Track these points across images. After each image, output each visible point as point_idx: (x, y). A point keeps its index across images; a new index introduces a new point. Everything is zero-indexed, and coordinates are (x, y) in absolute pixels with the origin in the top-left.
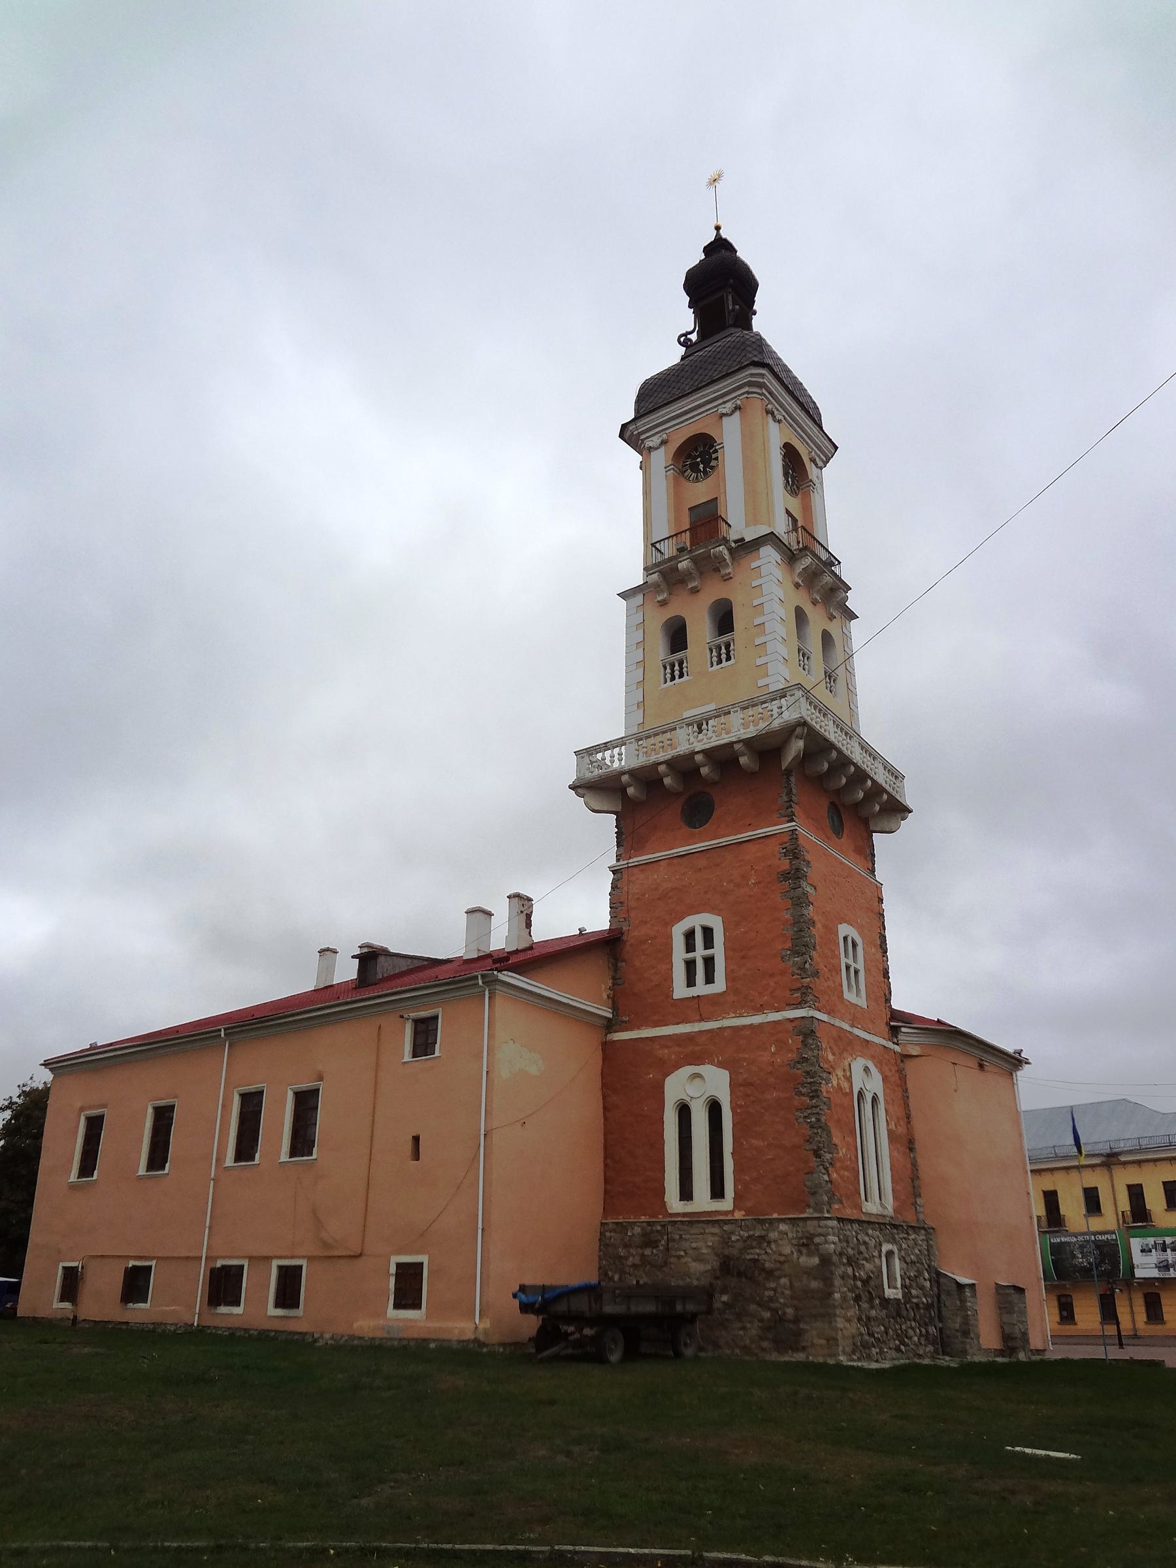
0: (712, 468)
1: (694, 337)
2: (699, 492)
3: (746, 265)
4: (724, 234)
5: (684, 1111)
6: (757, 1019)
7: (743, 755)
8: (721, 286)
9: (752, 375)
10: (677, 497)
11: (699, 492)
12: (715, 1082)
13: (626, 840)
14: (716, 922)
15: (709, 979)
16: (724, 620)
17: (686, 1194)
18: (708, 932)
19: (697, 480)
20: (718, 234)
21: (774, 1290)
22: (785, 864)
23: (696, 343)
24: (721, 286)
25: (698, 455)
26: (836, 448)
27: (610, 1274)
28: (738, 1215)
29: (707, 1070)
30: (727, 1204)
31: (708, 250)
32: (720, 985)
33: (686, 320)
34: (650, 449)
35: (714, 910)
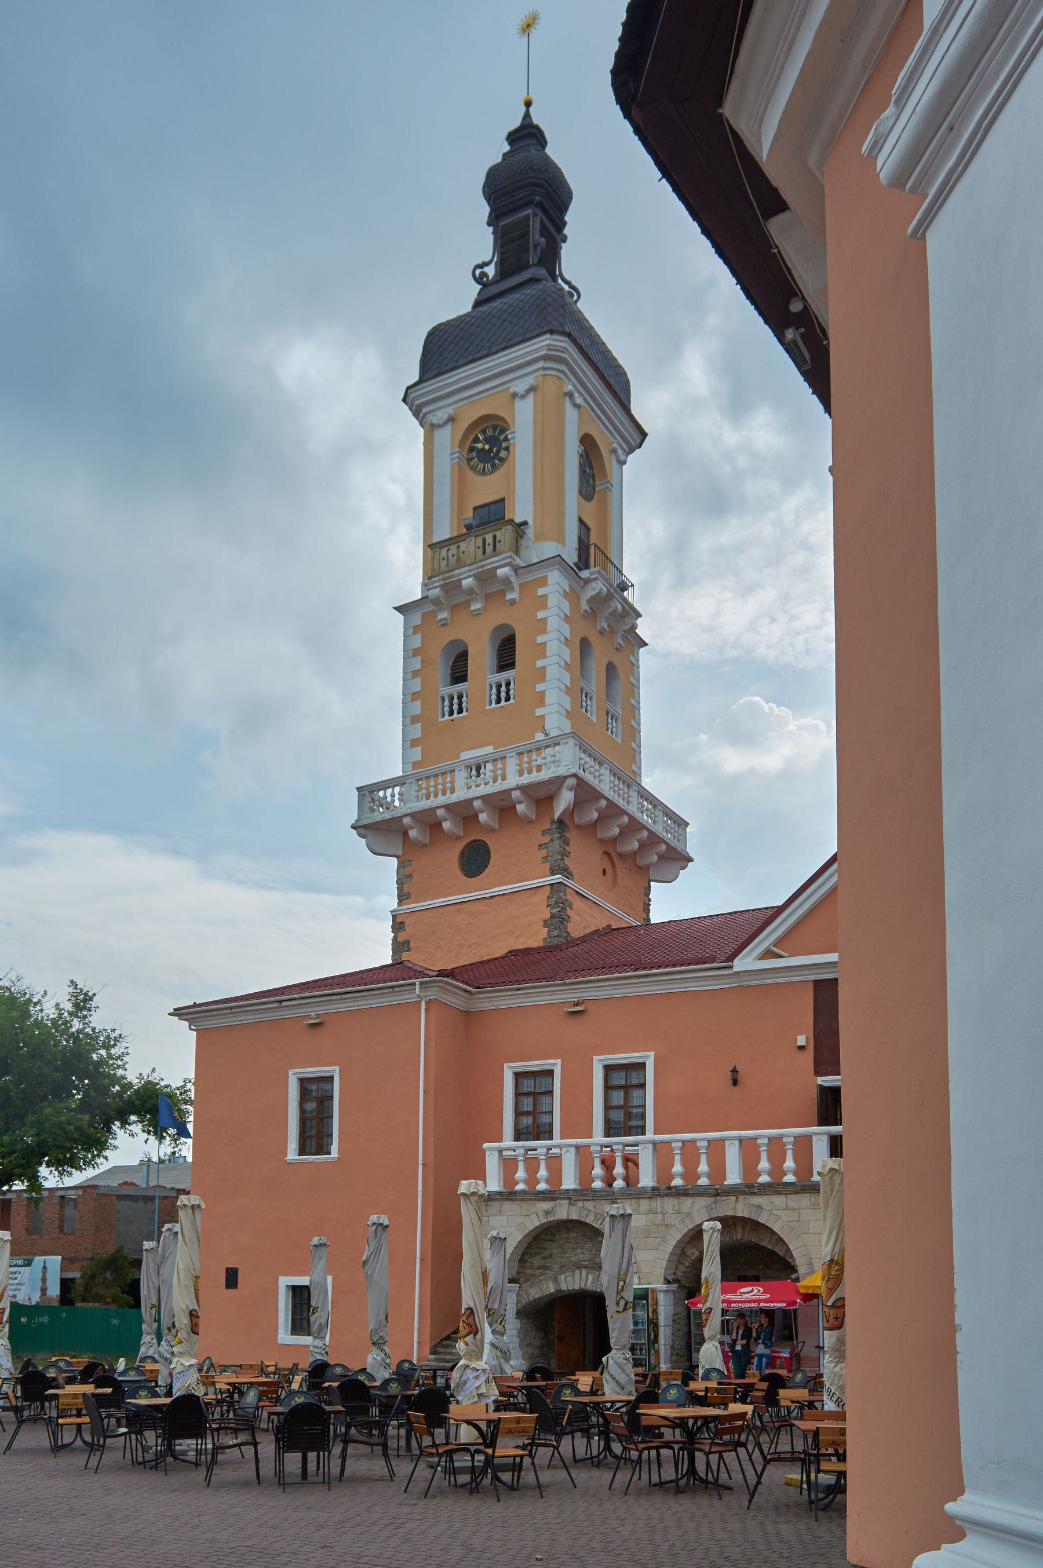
0: (501, 460)
2: (485, 489)
3: (560, 172)
10: (461, 491)
11: (485, 489)
19: (483, 473)
20: (527, 115)
23: (495, 282)
25: (487, 444)
31: (513, 138)
33: (481, 244)
34: (433, 426)
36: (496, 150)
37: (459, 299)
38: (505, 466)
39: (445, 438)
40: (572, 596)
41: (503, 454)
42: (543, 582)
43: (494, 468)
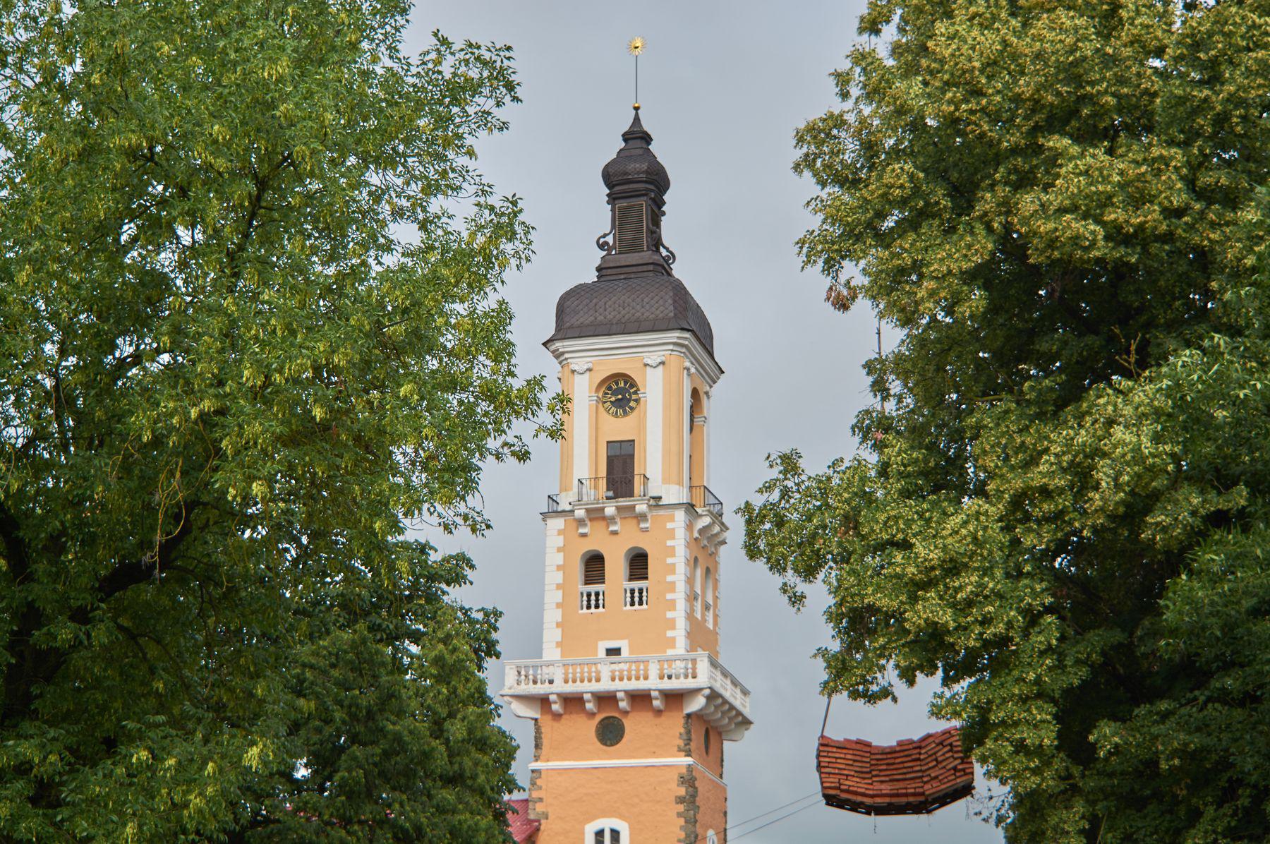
0: (632, 408)
1: (610, 239)
2: (618, 428)
4: (647, 126)
16: (638, 564)
19: (616, 415)
20: (637, 119)
24: (637, 184)
31: (627, 137)
35: (621, 817)
38: (635, 412)
40: (689, 527)
41: (632, 404)
42: (672, 519)
43: (626, 413)
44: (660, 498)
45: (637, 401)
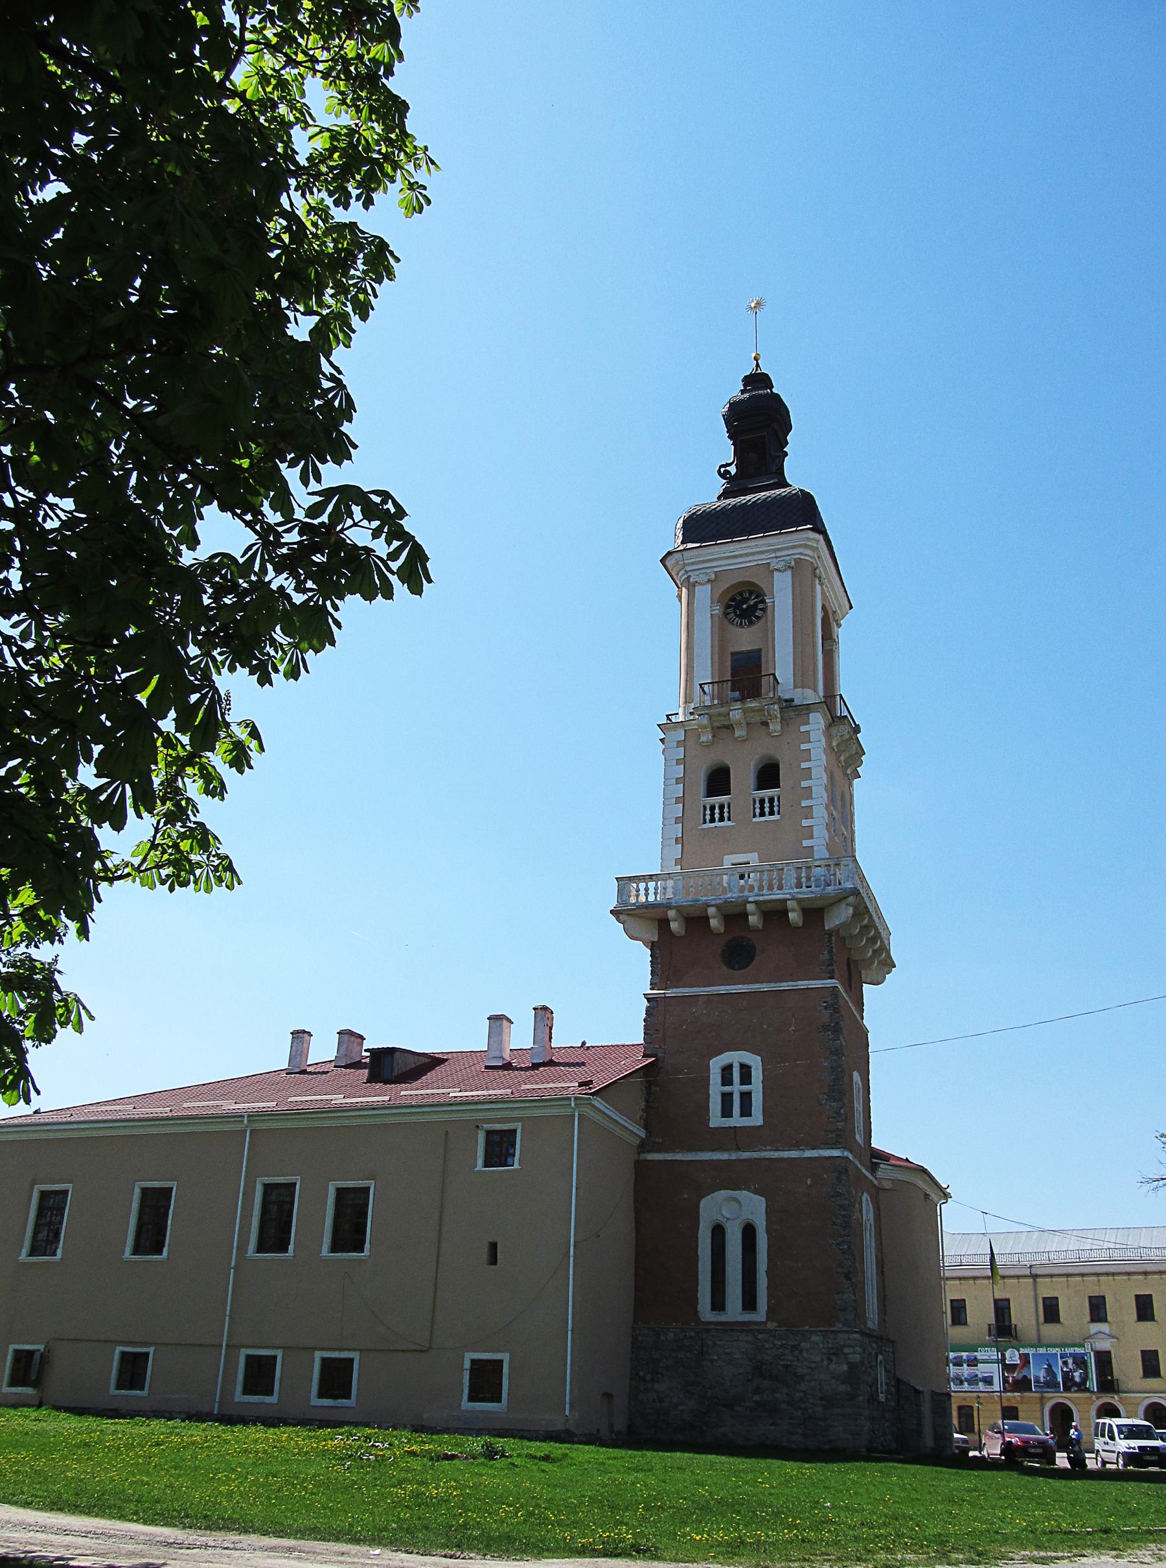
0: (758, 618)
1: (733, 470)
5: (718, 1232)
6: (794, 1154)
7: (793, 910)
8: (758, 422)
9: (808, 539)
12: (751, 1207)
13: (662, 971)
14: (755, 1061)
15: (746, 1111)
16: (768, 775)
17: (718, 1304)
18: (746, 1071)
21: (805, 1392)
22: (825, 1016)
24: (758, 422)
26: (851, 607)
27: (642, 1374)
28: (770, 1326)
29: (744, 1195)
30: (761, 1314)
31: (747, 380)
32: (757, 1119)
33: (726, 452)
36: (734, 390)
37: (708, 492)
38: (763, 620)
39: (704, 593)
43: (751, 623)
44: (792, 700)
45: (764, 610)
